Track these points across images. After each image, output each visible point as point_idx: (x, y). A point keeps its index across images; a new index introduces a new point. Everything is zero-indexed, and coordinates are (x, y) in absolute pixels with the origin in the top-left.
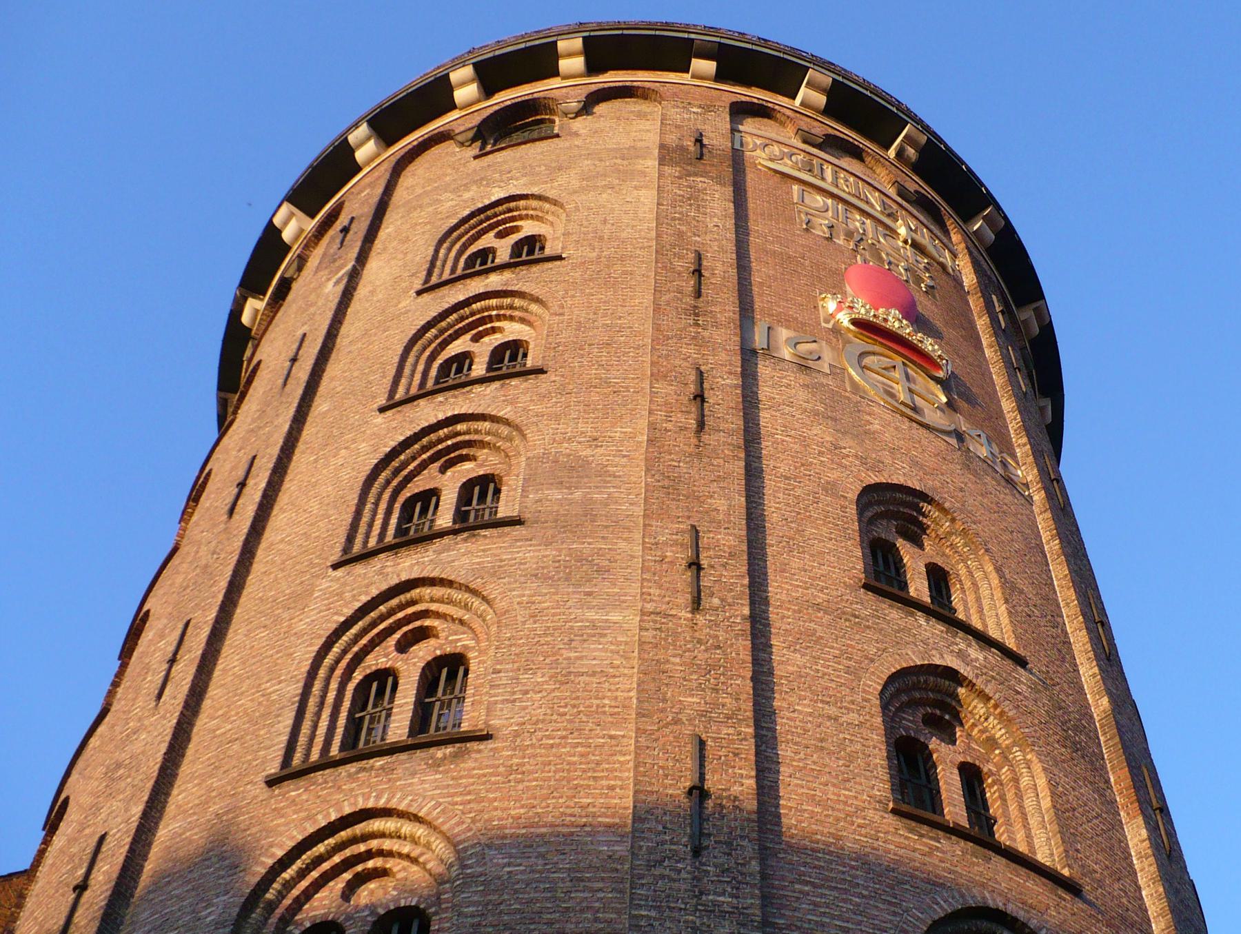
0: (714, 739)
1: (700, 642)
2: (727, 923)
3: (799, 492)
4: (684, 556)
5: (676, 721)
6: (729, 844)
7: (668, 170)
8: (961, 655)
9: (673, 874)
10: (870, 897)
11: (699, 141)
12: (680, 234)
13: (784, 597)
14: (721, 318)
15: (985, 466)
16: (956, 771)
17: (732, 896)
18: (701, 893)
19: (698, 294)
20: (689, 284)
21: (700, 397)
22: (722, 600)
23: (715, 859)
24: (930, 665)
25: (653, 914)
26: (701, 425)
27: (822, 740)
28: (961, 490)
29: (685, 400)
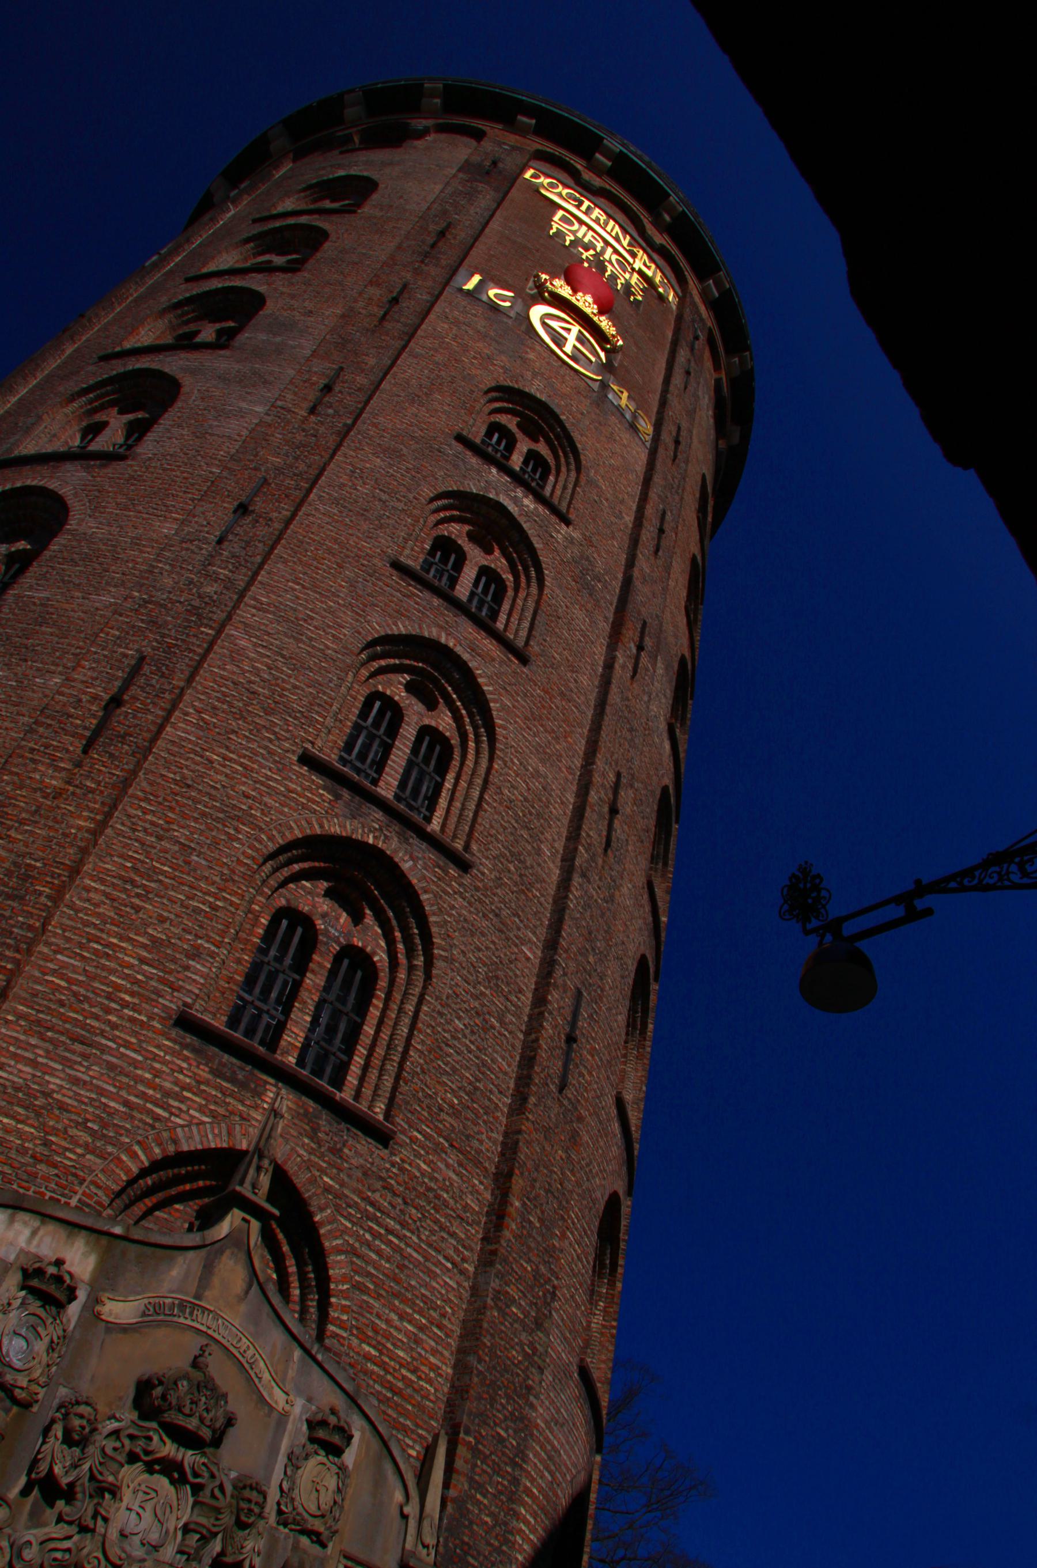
0: (277, 484)
1: (304, 430)
2: (216, 585)
3: (443, 373)
4: (323, 382)
5: (256, 469)
6: (248, 543)
7: (461, 175)
8: (516, 500)
9: (196, 550)
10: (344, 606)
11: (494, 163)
12: (445, 212)
13: (390, 426)
14: (444, 263)
15: (614, 410)
16: (477, 569)
17: (230, 571)
18: (209, 564)
19: (433, 246)
20: (430, 241)
21: (395, 301)
22: (335, 411)
23: (233, 546)
24: (484, 496)
25: (167, 567)
26: (384, 317)
27: (365, 510)
28: (582, 414)
29: (385, 300)
